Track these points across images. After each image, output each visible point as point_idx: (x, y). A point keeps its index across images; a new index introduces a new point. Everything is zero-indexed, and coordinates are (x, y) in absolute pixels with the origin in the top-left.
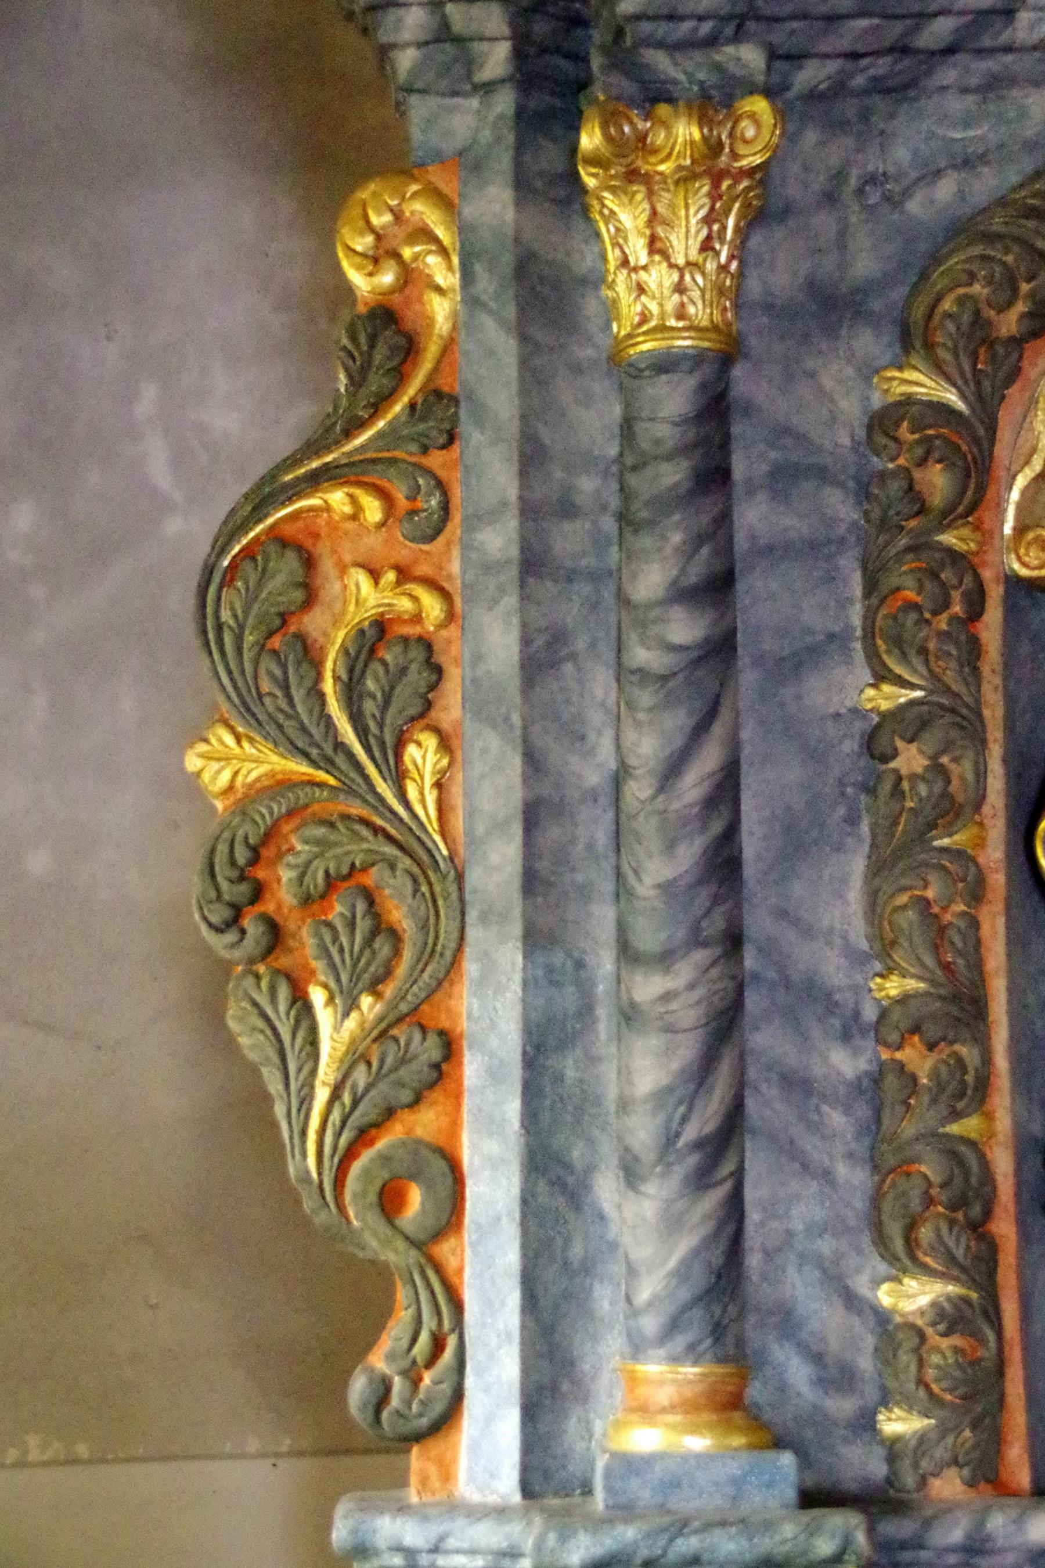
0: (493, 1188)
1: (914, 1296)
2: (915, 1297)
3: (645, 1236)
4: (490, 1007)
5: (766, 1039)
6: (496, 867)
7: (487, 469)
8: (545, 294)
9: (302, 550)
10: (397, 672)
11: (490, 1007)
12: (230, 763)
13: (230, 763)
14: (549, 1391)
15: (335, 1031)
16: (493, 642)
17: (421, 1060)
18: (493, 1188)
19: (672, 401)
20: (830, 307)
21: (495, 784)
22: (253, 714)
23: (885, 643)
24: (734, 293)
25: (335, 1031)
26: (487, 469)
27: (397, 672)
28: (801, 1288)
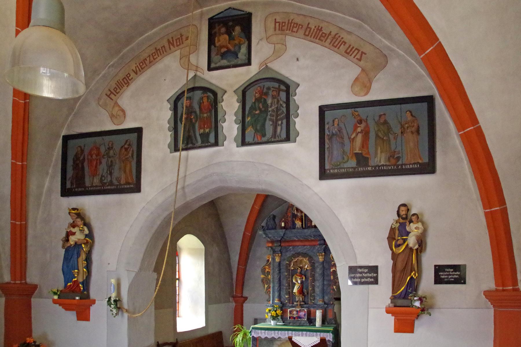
0: (271, 292)
1: (287, 297)
2: (287, 297)
3: (277, 294)
4: (271, 285)
5: (282, 287)
6: (272, 280)
7: (271, 266)
8: (274, 259)
9: (265, 269)
10: (268, 273)
11: (271, 285)
12: (262, 276)
13: (262, 276)
14: (273, 300)
15: (266, 286)
16: (271, 272)
17: (269, 287)
18: (271, 292)
19: (277, 264)
20: (284, 260)
21: (272, 277)
22: (263, 274)
23: (286, 272)
24: (280, 259)
25: (266, 286)
26: (271, 266)
27: (268, 273)
28: (283, 296)
